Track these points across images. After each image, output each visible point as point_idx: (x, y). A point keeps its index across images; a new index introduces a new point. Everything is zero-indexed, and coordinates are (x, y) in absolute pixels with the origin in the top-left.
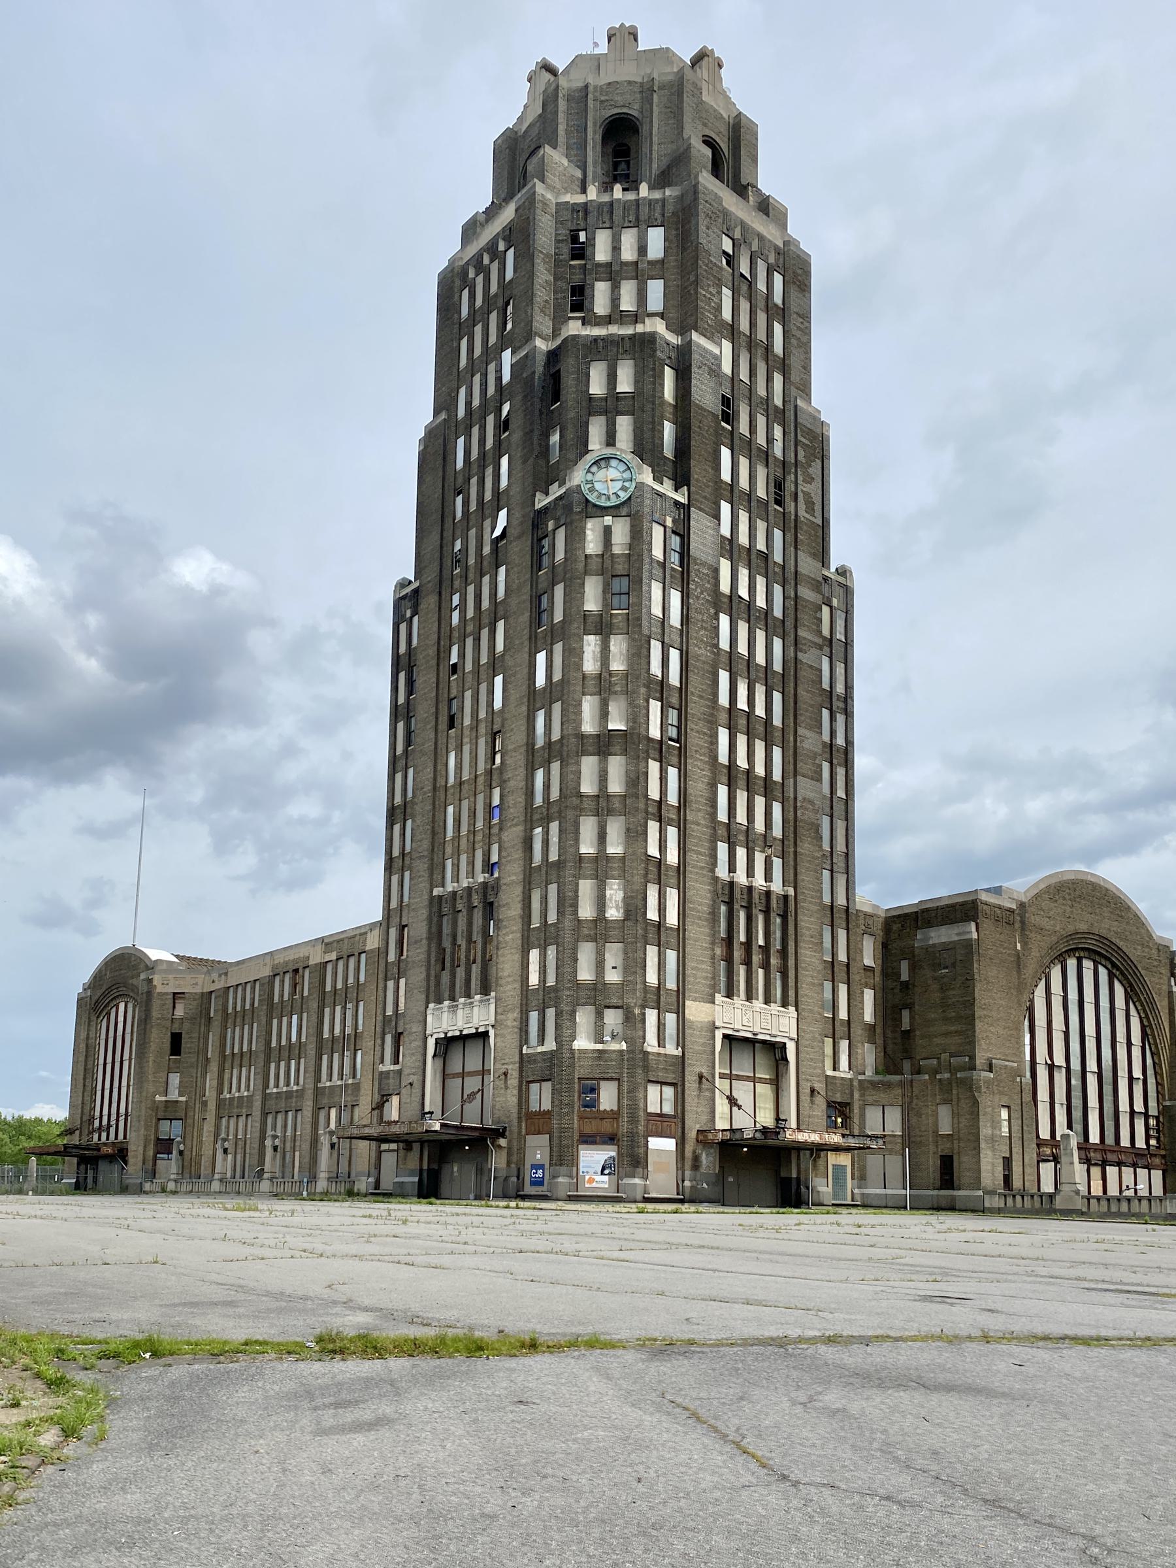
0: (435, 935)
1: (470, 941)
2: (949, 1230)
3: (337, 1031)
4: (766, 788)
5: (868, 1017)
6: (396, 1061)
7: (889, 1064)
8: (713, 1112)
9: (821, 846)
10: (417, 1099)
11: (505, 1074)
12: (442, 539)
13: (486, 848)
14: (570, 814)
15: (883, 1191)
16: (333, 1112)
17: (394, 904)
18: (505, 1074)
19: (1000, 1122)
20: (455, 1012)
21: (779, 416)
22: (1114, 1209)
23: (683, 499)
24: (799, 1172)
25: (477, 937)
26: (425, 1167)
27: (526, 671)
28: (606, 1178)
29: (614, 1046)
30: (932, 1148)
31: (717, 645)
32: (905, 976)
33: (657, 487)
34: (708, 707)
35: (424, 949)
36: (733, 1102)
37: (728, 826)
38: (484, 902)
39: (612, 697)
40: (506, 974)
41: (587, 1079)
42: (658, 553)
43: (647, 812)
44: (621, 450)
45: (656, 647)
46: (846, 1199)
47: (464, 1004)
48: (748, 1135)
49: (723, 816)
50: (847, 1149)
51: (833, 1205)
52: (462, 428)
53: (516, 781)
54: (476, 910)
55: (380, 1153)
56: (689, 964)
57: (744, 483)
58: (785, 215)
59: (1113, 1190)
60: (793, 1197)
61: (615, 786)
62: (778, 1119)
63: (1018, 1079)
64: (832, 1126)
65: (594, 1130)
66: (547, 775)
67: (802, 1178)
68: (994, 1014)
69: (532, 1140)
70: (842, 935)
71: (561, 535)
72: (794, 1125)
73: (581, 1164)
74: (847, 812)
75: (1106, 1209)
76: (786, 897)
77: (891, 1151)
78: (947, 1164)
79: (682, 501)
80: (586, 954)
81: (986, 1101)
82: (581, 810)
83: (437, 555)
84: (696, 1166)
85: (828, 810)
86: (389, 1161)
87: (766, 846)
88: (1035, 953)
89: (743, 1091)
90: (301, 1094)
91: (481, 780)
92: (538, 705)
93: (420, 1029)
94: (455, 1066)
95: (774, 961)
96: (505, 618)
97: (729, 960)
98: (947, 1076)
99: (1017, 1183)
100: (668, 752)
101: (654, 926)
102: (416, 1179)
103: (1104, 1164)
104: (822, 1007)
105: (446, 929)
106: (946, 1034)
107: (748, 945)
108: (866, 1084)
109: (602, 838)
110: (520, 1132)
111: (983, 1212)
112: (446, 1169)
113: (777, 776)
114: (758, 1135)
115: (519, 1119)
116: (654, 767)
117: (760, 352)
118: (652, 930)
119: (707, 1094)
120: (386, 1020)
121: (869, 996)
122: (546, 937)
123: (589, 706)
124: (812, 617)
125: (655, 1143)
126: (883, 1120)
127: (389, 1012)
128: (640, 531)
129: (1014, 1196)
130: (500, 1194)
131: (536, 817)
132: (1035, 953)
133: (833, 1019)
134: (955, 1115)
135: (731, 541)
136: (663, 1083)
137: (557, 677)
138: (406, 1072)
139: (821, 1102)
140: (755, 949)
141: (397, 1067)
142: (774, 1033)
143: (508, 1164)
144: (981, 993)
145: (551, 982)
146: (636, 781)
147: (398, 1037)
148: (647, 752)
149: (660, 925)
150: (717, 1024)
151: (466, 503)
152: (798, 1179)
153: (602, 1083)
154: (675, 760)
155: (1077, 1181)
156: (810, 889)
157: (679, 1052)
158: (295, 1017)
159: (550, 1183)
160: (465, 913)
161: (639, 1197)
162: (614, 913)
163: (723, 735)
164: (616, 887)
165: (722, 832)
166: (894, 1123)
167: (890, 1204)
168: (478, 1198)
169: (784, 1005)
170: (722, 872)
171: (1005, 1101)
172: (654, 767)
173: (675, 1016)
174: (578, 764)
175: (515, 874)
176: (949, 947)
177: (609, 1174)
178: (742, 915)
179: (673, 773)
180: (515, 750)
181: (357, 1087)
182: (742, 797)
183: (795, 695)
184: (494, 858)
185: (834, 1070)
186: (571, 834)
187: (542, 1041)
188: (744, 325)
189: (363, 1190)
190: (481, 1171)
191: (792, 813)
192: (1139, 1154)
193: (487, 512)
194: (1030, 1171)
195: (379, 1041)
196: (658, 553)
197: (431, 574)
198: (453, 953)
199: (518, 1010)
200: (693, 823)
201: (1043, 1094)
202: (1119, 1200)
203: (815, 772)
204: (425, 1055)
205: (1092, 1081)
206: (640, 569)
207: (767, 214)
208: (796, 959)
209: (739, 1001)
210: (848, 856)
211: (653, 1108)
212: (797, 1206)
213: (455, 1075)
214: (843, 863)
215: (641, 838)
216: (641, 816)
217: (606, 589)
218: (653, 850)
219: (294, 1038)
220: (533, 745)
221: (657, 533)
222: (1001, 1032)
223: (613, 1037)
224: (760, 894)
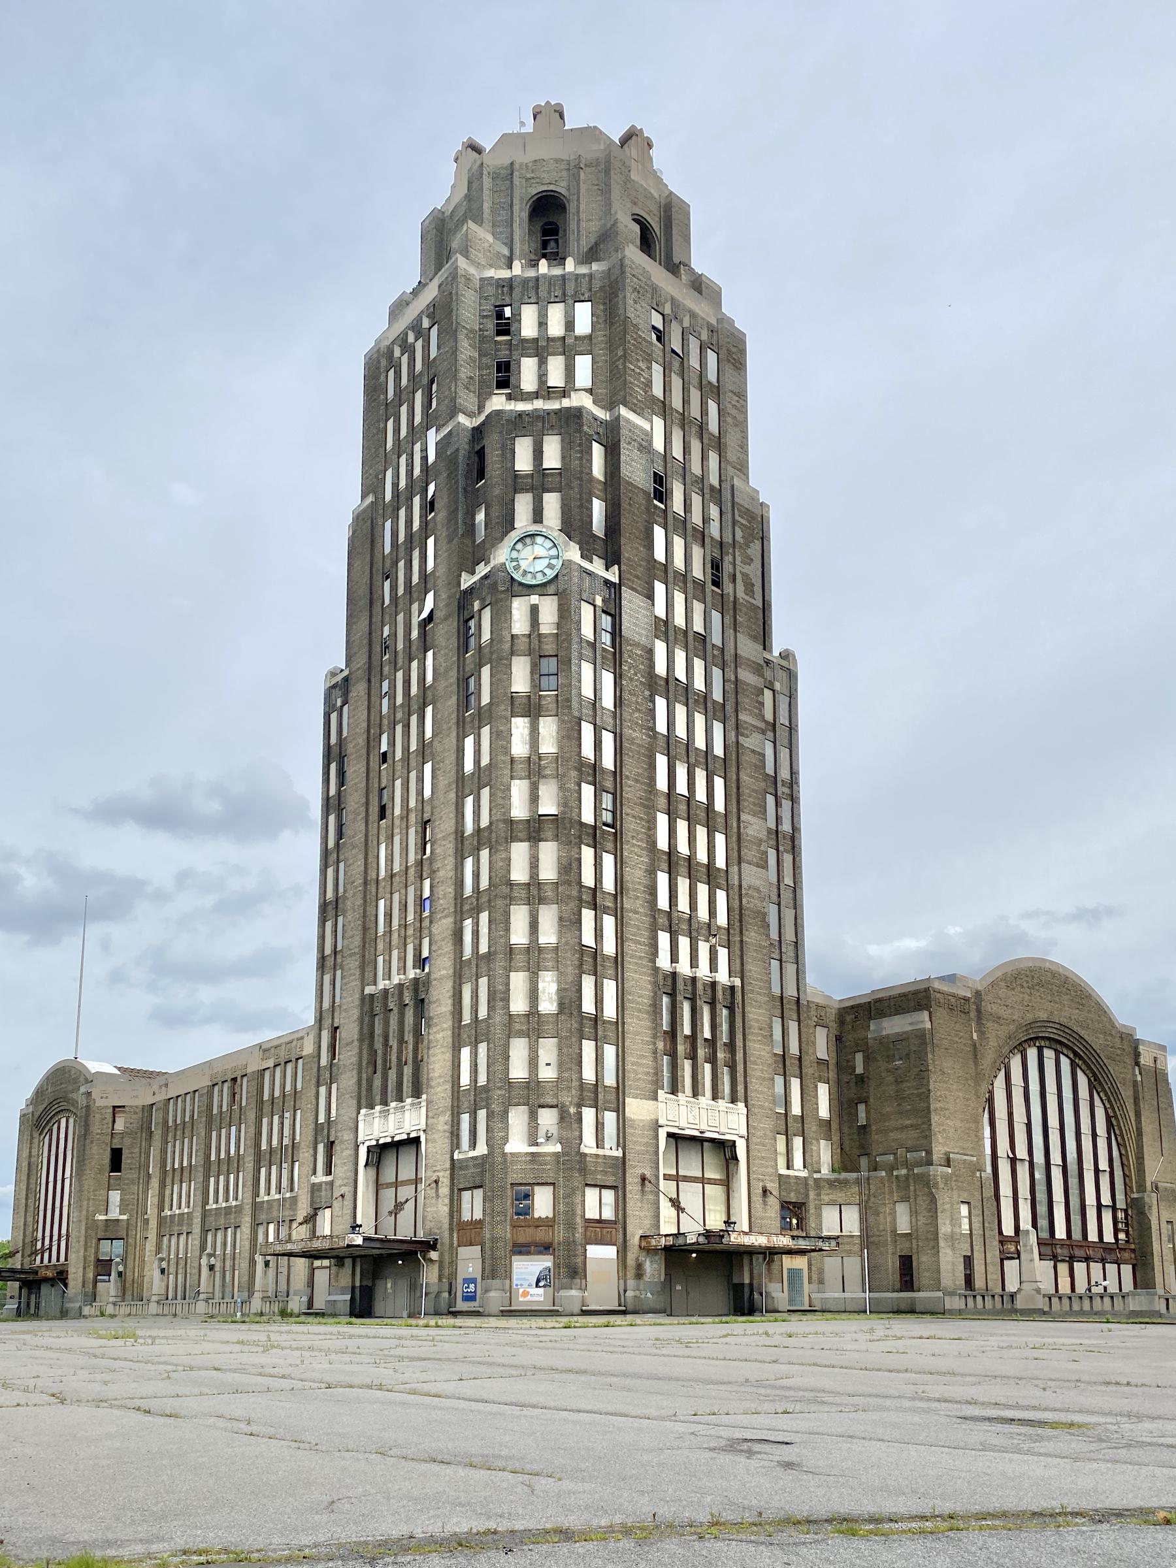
5: (824, 1112)
7: (845, 1162)
9: (768, 936)
10: (348, 1211)
11: (436, 1182)
12: (370, 625)
13: (417, 942)
14: (500, 903)
15: (842, 1295)
18: (436, 1182)
19: (959, 1219)
20: (386, 1117)
21: (716, 495)
23: (615, 579)
24: (752, 1278)
26: (358, 1284)
27: (454, 756)
28: (541, 1291)
30: (890, 1249)
31: (653, 729)
33: (586, 564)
36: (676, 1203)
37: (669, 914)
39: (541, 781)
40: (436, 1075)
41: (521, 1184)
42: (587, 632)
43: (580, 900)
44: (548, 527)
45: (587, 730)
46: (803, 1305)
47: (395, 1108)
49: (663, 903)
50: (802, 1252)
52: (389, 511)
53: (446, 871)
54: (407, 1008)
56: (629, 1059)
57: (679, 562)
58: (720, 294)
60: (746, 1305)
61: (548, 872)
63: (978, 1174)
64: (786, 1228)
65: (529, 1240)
66: (477, 862)
67: (755, 1282)
68: (951, 1106)
69: (465, 1252)
71: (487, 615)
73: (515, 1277)
74: (795, 899)
76: (732, 988)
78: (906, 1264)
79: (613, 580)
80: (519, 1049)
81: (944, 1198)
83: (366, 641)
84: (639, 1275)
89: (690, 1195)
91: (412, 871)
92: (467, 791)
96: (433, 703)
97: (673, 1055)
98: (904, 1172)
99: (979, 1283)
100: (602, 838)
102: (348, 1297)
103: (1071, 1260)
104: (774, 1102)
106: (903, 1128)
107: (693, 1038)
108: (823, 1184)
110: (451, 1245)
112: (380, 1284)
113: (721, 862)
115: (451, 1230)
116: (587, 853)
117: (694, 429)
118: (588, 1023)
119: (651, 1197)
122: (477, 1033)
123: (519, 790)
124: (755, 693)
125: (593, 1251)
126: (838, 1219)
128: (568, 611)
130: (432, 1311)
131: (466, 907)
133: (786, 1114)
134: (914, 1213)
135: (666, 622)
137: (485, 761)
139: (774, 1203)
140: (700, 1042)
142: (723, 1130)
143: (440, 1279)
145: (482, 1080)
146: (570, 868)
148: (580, 837)
149: (596, 1019)
150: (661, 1122)
151: (394, 588)
152: (751, 1285)
153: (536, 1188)
154: (610, 846)
156: (757, 980)
157: (619, 1153)
159: (482, 1298)
160: (396, 1011)
161: (577, 1310)
162: (548, 1006)
163: (662, 820)
165: (662, 920)
166: (852, 1223)
170: (663, 961)
171: (965, 1196)
172: (587, 853)
174: (508, 851)
175: (444, 968)
176: (901, 1038)
177: (544, 1286)
178: (686, 1007)
179: (608, 860)
180: (444, 838)
182: (683, 884)
183: (738, 780)
186: (501, 924)
187: (473, 1145)
188: (677, 403)
190: (414, 1286)
191: (737, 902)
193: (415, 595)
196: (587, 632)
197: (361, 661)
198: (385, 1054)
199: (449, 1113)
201: (1005, 1189)
205: (1057, 1174)
206: (569, 648)
207: (700, 293)
208: (745, 1053)
209: (684, 1097)
211: (592, 1213)
217: (535, 669)
220: (463, 832)
221: (587, 612)
222: (958, 1124)
223: (548, 1138)
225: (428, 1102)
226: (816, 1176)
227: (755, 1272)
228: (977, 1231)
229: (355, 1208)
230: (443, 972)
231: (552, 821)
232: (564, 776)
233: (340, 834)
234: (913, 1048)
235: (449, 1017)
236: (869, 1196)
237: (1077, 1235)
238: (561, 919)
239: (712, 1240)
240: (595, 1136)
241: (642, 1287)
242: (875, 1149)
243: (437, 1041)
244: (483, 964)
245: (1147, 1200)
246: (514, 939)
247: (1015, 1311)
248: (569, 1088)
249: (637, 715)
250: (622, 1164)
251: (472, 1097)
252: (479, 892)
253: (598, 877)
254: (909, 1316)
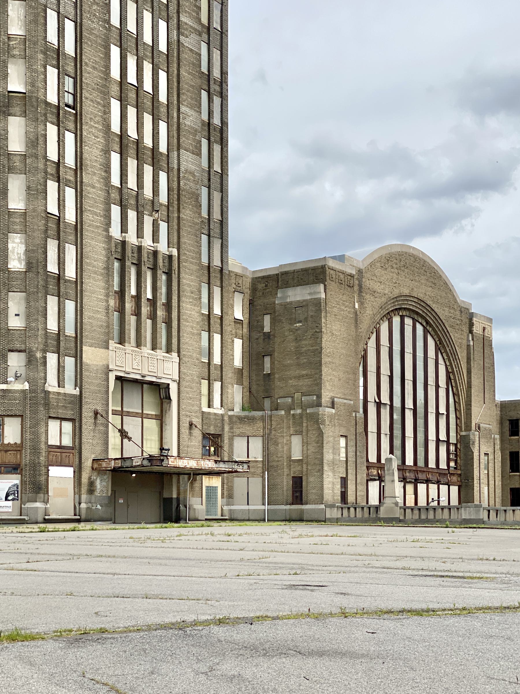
2: (300, 536)
4: (153, 159)
5: (238, 362)
7: (253, 402)
8: (106, 443)
22: (423, 517)
29: (18, 386)
32: (267, 329)
34: (101, 78)
36: (123, 434)
37: (120, 190)
39: (10, 60)
43: (46, 172)
46: (216, 515)
48: (137, 462)
50: (218, 473)
51: (206, 520)
56: (86, 313)
59: (422, 502)
62: (162, 449)
64: (206, 454)
67: (181, 497)
70: (217, 291)
72: (175, 453)
75: (417, 517)
76: (170, 257)
77: (254, 474)
78: (298, 484)
85: (206, 182)
87: (153, 210)
88: (369, 311)
89: (132, 426)
95: (161, 313)
97: (121, 310)
99: (351, 498)
101: (54, 278)
103: (416, 482)
104: (200, 353)
107: (138, 298)
111: (325, 521)
114: (146, 463)
121: (238, 344)
125: (55, 471)
129: (349, 508)
132: (369, 311)
133: (209, 364)
134: (305, 444)
136: (62, 419)
139: (197, 434)
142: (159, 375)
144: (326, 342)
148: (45, 115)
150: (111, 367)
152: (178, 499)
154: (71, 126)
155: (397, 495)
157: (77, 392)
164: (18, 240)
165: (115, 195)
167: (251, 518)
169: (169, 350)
170: (115, 231)
171: (343, 432)
172: (52, 130)
173: (73, 359)
176: (302, 305)
178: (133, 271)
179: (70, 138)
185: (209, 407)
192: (442, 474)
194: (361, 488)
200: (89, 185)
201: (372, 427)
202: (427, 509)
203: (196, 147)
205: (409, 415)
209: (130, 347)
210: (223, 223)
211: (54, 440)
212: (177, 521)
214: (217, 229)
216: (40, 176)
218: (53, 208)
222: (341, 375)
223: (17, 378)
224: (148, 253)
226: (231, 413)
227: (181, 488)
228: (351, 459)
231: (20, 98)
232: (31, 57)
234: (311, 313)
236: (271, 430)
237: (421, 463)
239: (154, 462)
240: (56, 377)
241: (93, 501)
242: (277, 393)
245: (472, 437)
247: (380, 519)
249: (95, 7)
250: (79, 401)
253: (61, 153)
254: (298, 523)
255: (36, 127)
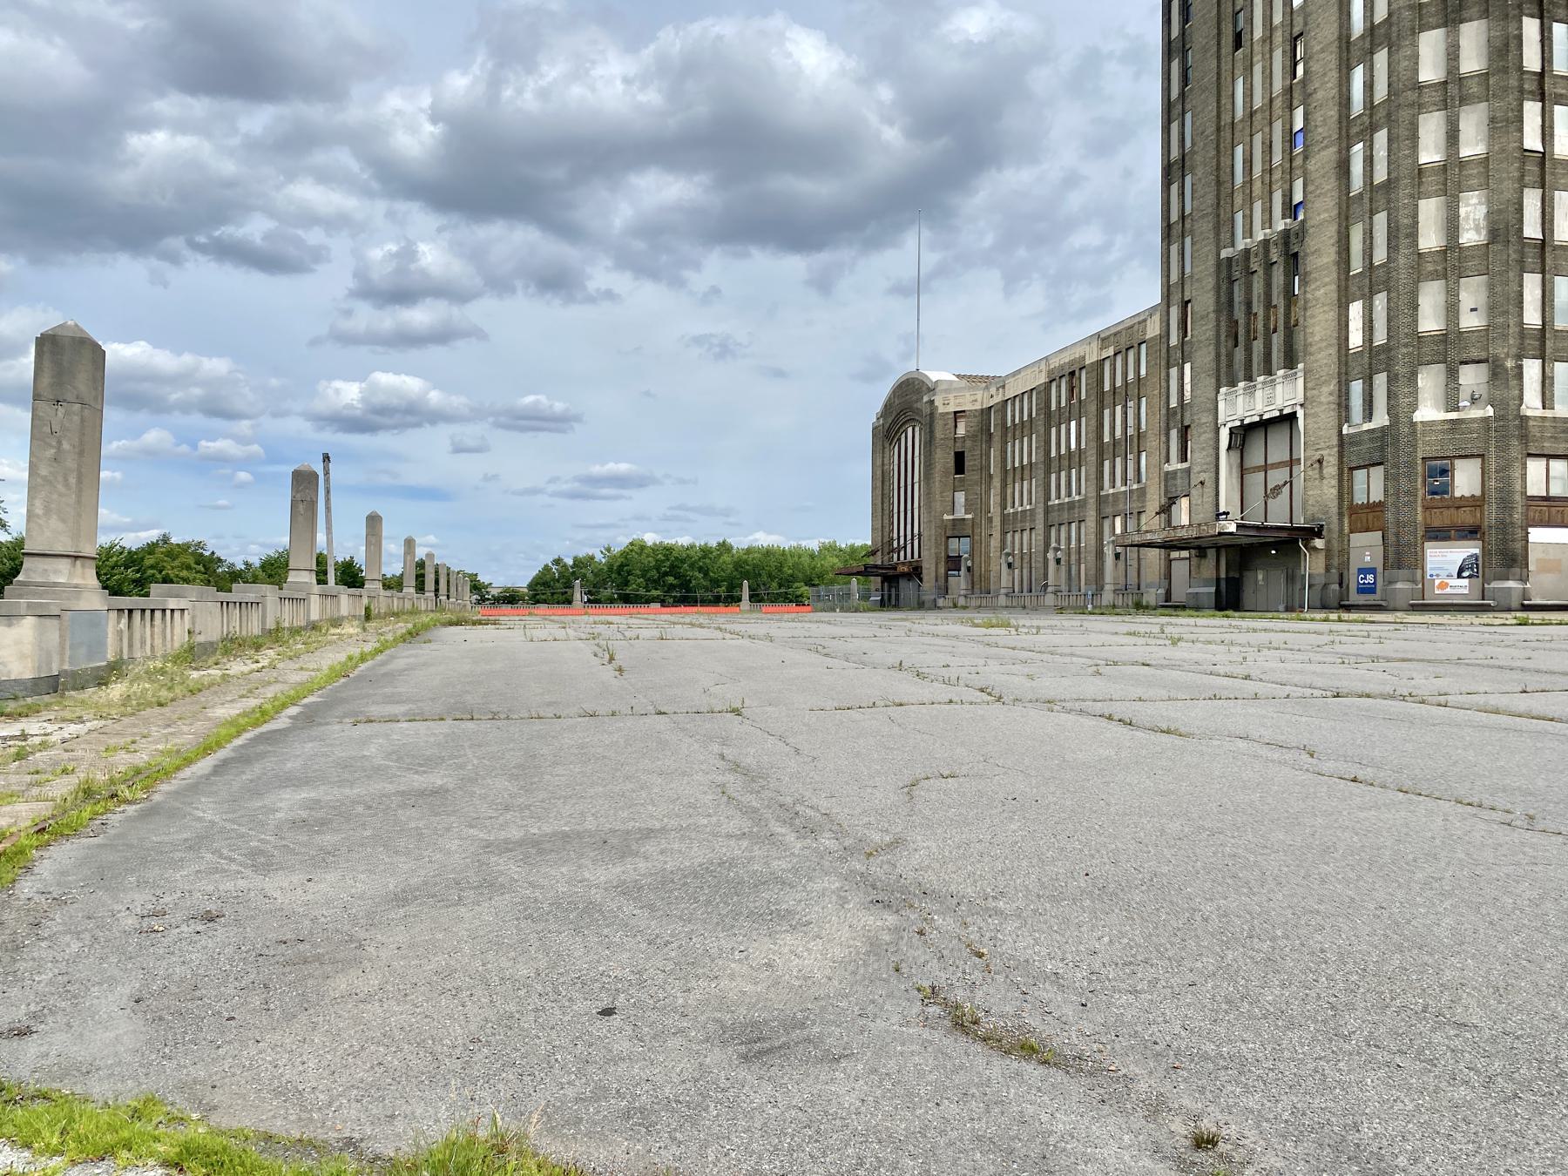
0: (1225, 305)
1: (1268, 305)
3: (1118, 433)
6: (1184, 458)
11: (1320, 462)
13: (1287, 186)
14: (1404, 114)
16: (1118, 521)
17: (1174, 277)
18: (1320, 462)
20: (1252, 394)
25: (1278, 299)
26: (1223, 575)
29: (1476, 413)
35: (1212, 325)
38: (1287, 253)
40: (1317, 338)
41: (1436, 458)
43: (1521, 91)
53: (1325, 90)
55: (1169, 561)
61: (1472, 62)
65: (1447, 522)
69: (1358, 539)
82: (1420, 106)
86: (1180, 570)
90: (1083, 504)
91: (1278, 103)
93: (1211, 418)
94: (1255, 457)
102: (1213, 589)
105: (1238, 296)
109: (1453, 137)
115: (1341, 514)
120: (1170, 413)
122: (1374, 281)
127: (1173, 404)
131: (1354, 130)
138: (1196, 469)
141: (1185, 465)
143: (1327, 569)
145: (1380, 338)
147: (1184, 431)
153: (1457, 462)
158: (1073, 424)
160: (1261, 272)
162: (1471, 236)
164: (1475, 201)
168: (1289, 609)
174: (1415, 45)
175: (1326, 211)
181: (1142, 492)
184: (1298, 197)
187: (1369, 414)
189: (1153, 603)
190: (1291, 578)
195: (1163, 439)
198: (1248, 324)
199: (1335, 381)
204: (1217, 449)
213: (1257, 469)
215: (1512, 128)
219: (1073, 446)
220: (1349, 36)
223: (1473, 400)
225: (1306, 372)
229: (1217, 494)
230: (1324, 216)
233: (1185, 80)
235: (1334, 268)
238: (1492, 120)
243: (1317, 300)
244: (1381, 200)
246: (1424, 158)
248: (1505, 336)
251: (1366, 360)
252: (1372, 107)
255: (1504, 29)
